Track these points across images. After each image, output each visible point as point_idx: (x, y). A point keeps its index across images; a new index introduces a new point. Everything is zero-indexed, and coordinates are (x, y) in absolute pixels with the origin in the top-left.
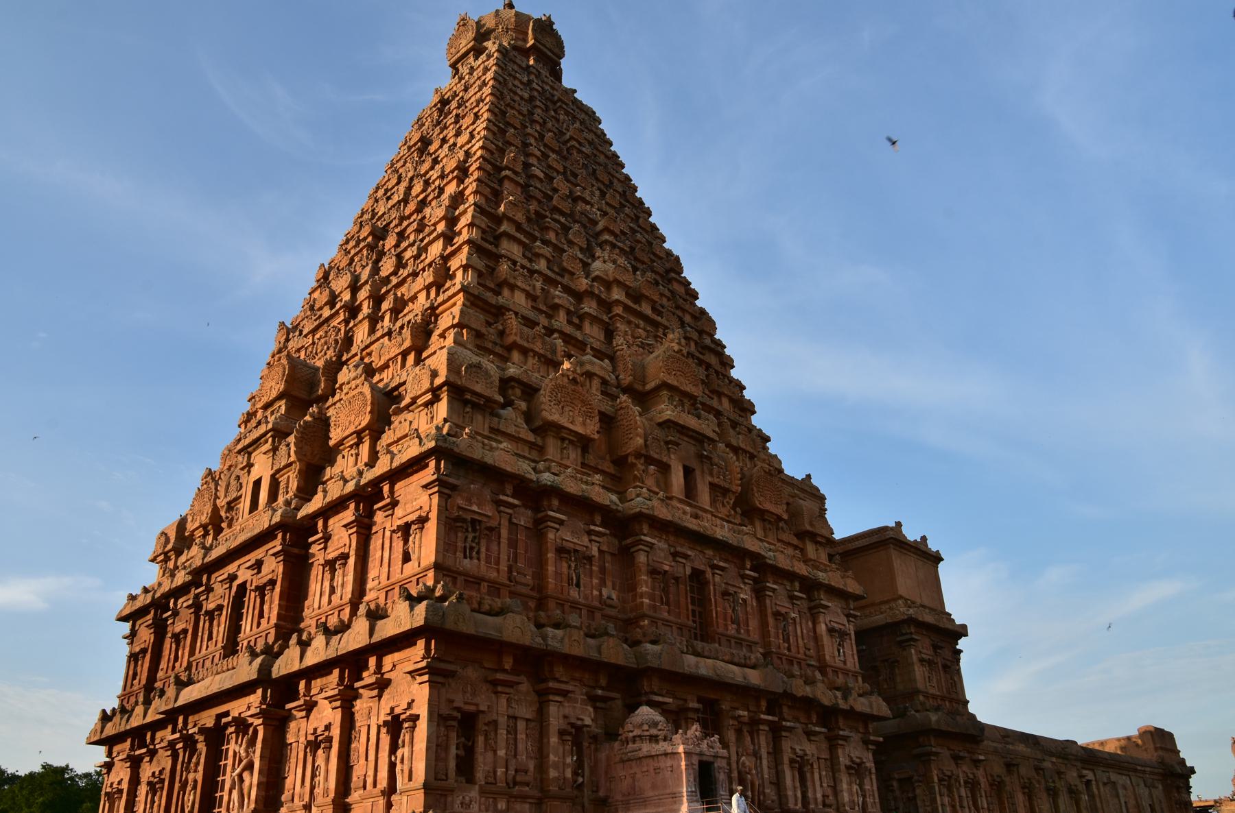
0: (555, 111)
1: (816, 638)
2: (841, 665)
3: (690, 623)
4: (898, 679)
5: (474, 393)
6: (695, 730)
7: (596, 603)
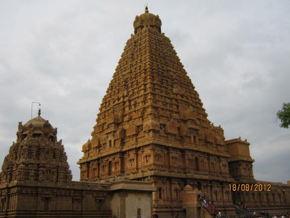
0: (161, 44)
1: (220, 167)
2: (225, 172)
3: (195, 168)
4: (238, 172)
5: (156, 130)
6: (197, 189)
7: (179, 166)
